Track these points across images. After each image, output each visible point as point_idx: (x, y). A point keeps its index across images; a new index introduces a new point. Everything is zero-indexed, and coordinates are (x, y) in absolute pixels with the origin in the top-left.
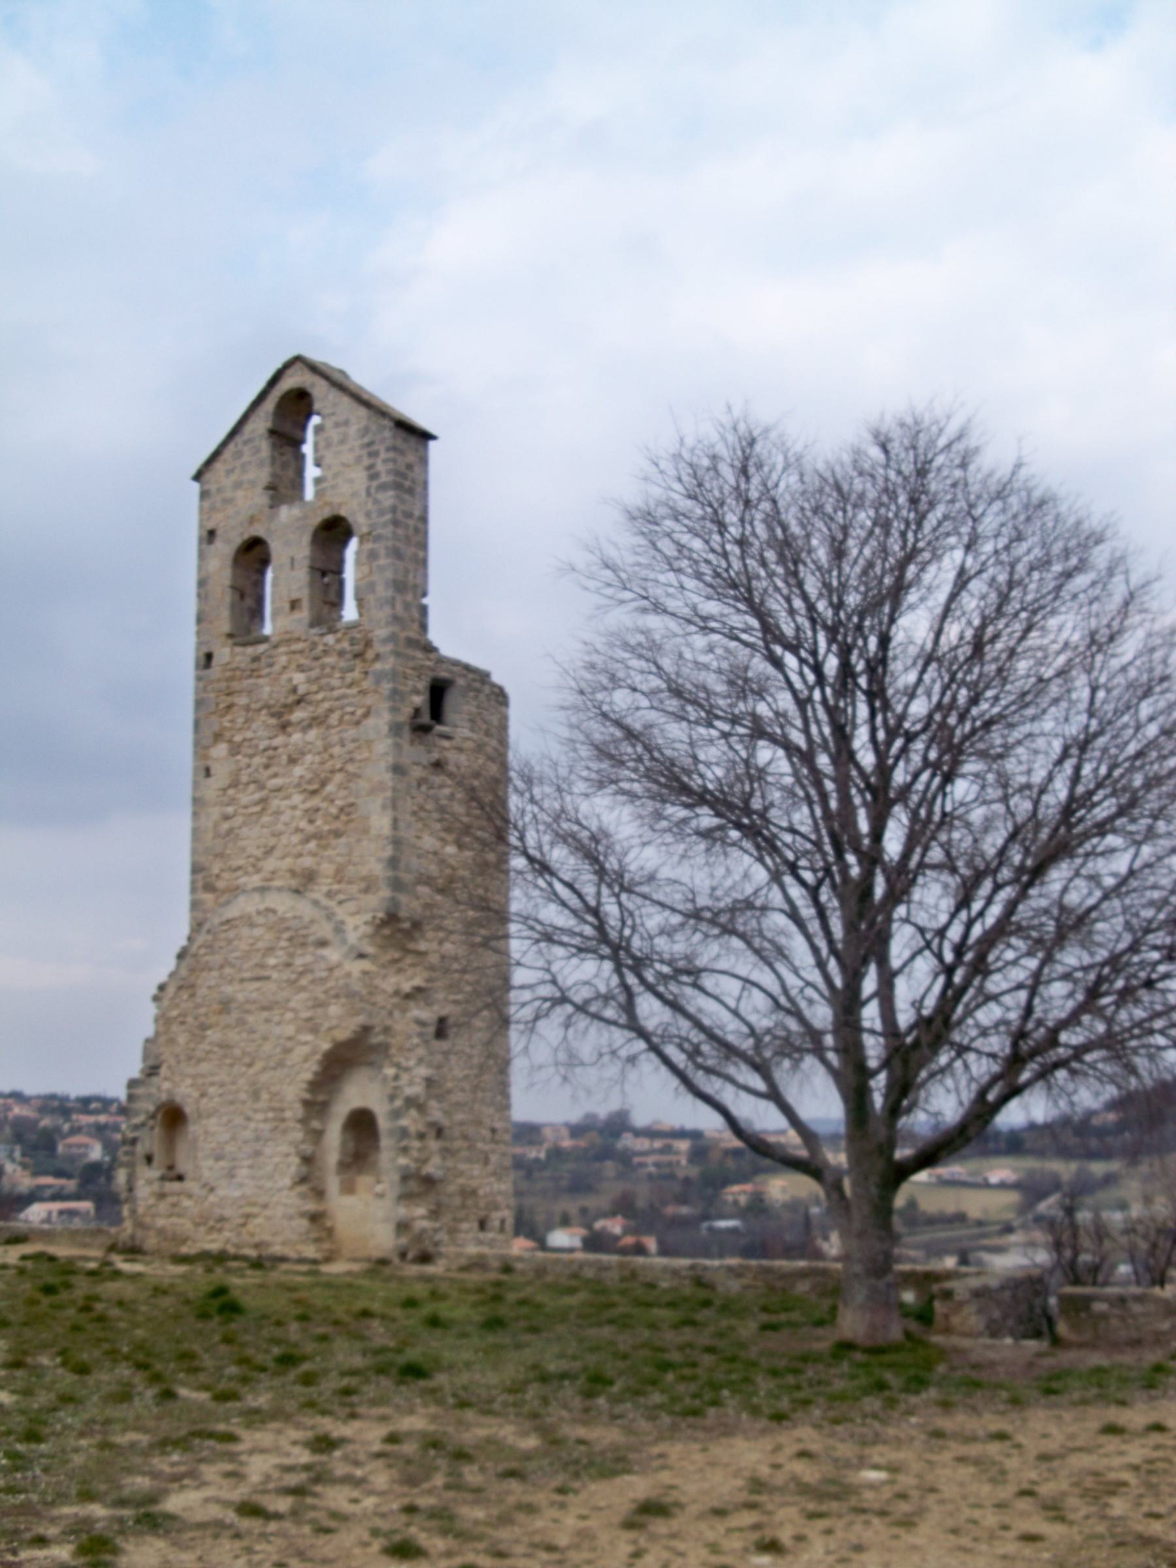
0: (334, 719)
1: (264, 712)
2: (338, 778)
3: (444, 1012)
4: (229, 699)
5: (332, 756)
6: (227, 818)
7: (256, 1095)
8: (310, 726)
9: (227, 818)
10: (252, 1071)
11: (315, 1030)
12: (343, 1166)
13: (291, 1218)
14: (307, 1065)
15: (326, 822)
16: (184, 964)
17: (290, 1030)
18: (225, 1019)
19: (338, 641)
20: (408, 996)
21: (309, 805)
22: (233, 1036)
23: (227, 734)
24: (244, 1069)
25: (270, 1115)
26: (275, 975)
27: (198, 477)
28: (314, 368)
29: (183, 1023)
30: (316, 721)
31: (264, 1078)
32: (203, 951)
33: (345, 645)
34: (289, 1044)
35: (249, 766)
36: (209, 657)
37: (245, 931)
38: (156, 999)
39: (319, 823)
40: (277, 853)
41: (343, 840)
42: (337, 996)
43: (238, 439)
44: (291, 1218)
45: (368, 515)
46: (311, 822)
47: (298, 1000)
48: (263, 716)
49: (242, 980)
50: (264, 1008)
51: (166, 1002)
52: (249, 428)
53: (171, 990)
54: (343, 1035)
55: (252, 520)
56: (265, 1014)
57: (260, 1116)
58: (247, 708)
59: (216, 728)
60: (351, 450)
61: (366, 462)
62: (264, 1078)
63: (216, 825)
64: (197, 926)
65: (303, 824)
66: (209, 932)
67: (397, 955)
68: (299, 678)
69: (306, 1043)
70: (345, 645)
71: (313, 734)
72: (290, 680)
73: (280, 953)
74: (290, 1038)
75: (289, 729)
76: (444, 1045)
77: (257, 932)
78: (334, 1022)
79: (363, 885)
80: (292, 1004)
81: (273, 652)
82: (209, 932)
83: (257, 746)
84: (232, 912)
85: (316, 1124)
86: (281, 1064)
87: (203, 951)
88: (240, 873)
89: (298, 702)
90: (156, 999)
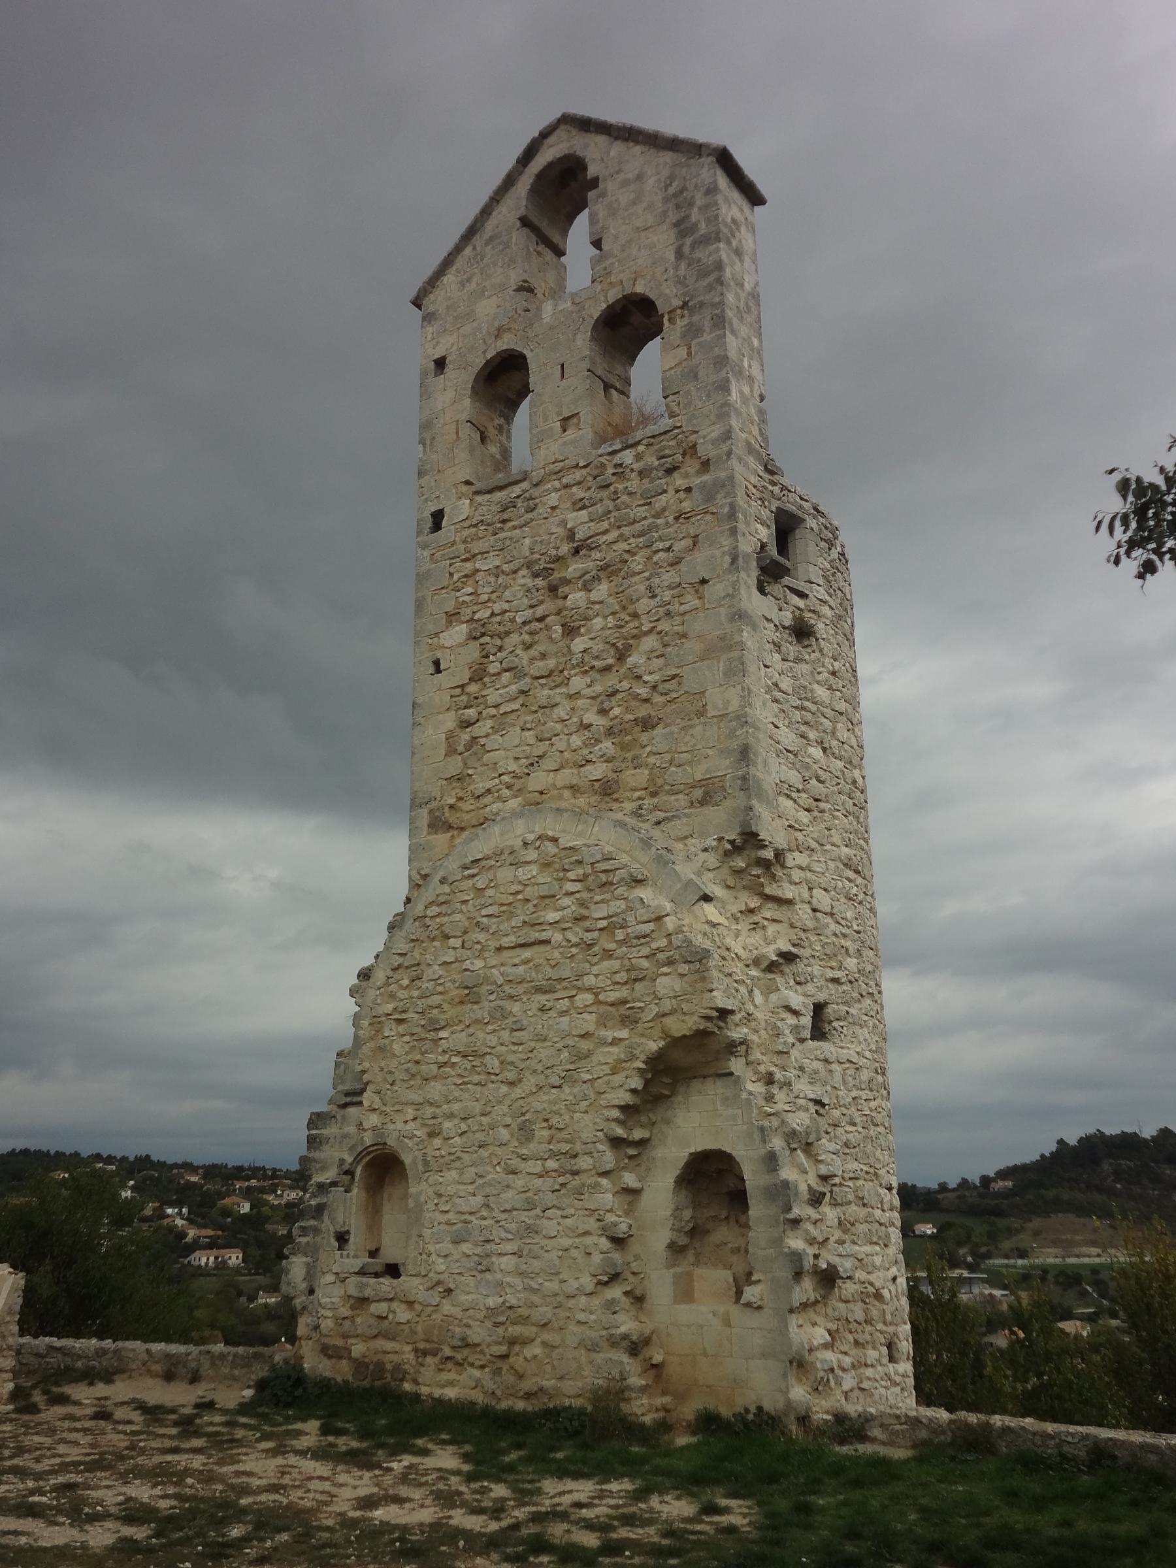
0: (637, 562)
1: (524, 572)
2: (650, 642)
3: (821, 997)
4: (469, 566)
5: (635, 616)
6: (466, 724)
7: (525, 1132)
8: (597, 579)
9: (466, 724)
10: (518, 1092)
11: (629, 1020)
12: (676, 1249)
13: (593, 1348)
14: (618, 1079)
15: (628, 710)
16: (401, 934)
17: (588, 1022)
18: (471, 1012)
19: (638, 457)
20: (772, 967)
21: (598, 688)
22: (484, 1037)
23: (466, 612)
24: (504, 1089)
25: (552, 1164)
26: (557, 937)
27: (417, 303)
28: (586, 125)
29: (400, 1021)
30: (607, 570)
31: (541, 1102)
32: (434, 910)
33: (652, 460)
34: (585, 1045)
35: (500, 649)
36: (438, 518)
37: (505, 874)
38: (353, 992)
39: (617, 711)
40: (548, 764)
41: (658, 731)
42: (670, 962)
43: (478, 241)
44: (593, 1348)
45: (680, 282)
46: (603, 712)
47: (598, 974)
48: (524, 578)
49: (500, 949)
50: (540, 990)
51: (372, 994)
52: (490, 226)
53: (379, 976)
54: (680, 1027)
55: (499, 332)
56: (542, 999)
57: (537, 1167)
58: (497, 572)
59: (450, 606)
60: (651, 206)
61: (673, 217)
62: (541, 1102)
63: (450, 736)
64: (419, 881)
65: (591, 717)
66: (443, 881)
67: (754, 903)
68: (577, 518)
69: (616, 1042)
70: (652, 460)
71: (602, 590)
72: (564, 523)
73: (566, 901)
74: (585, 1036)
75: (562, 590)
76: (826, 1048)
77: (523, 873)
78: (667, 1005)
79: (698, 793)
80: (590, 980)
81: (536, 492)
82: (443, 881)
83: (513, 621)
84: (481, 846)
85: (630, 1179)
86: (568, 1078)
87: (434, 910)
88: (488, 799)
89: (577, 551)
90: (353, 992)
